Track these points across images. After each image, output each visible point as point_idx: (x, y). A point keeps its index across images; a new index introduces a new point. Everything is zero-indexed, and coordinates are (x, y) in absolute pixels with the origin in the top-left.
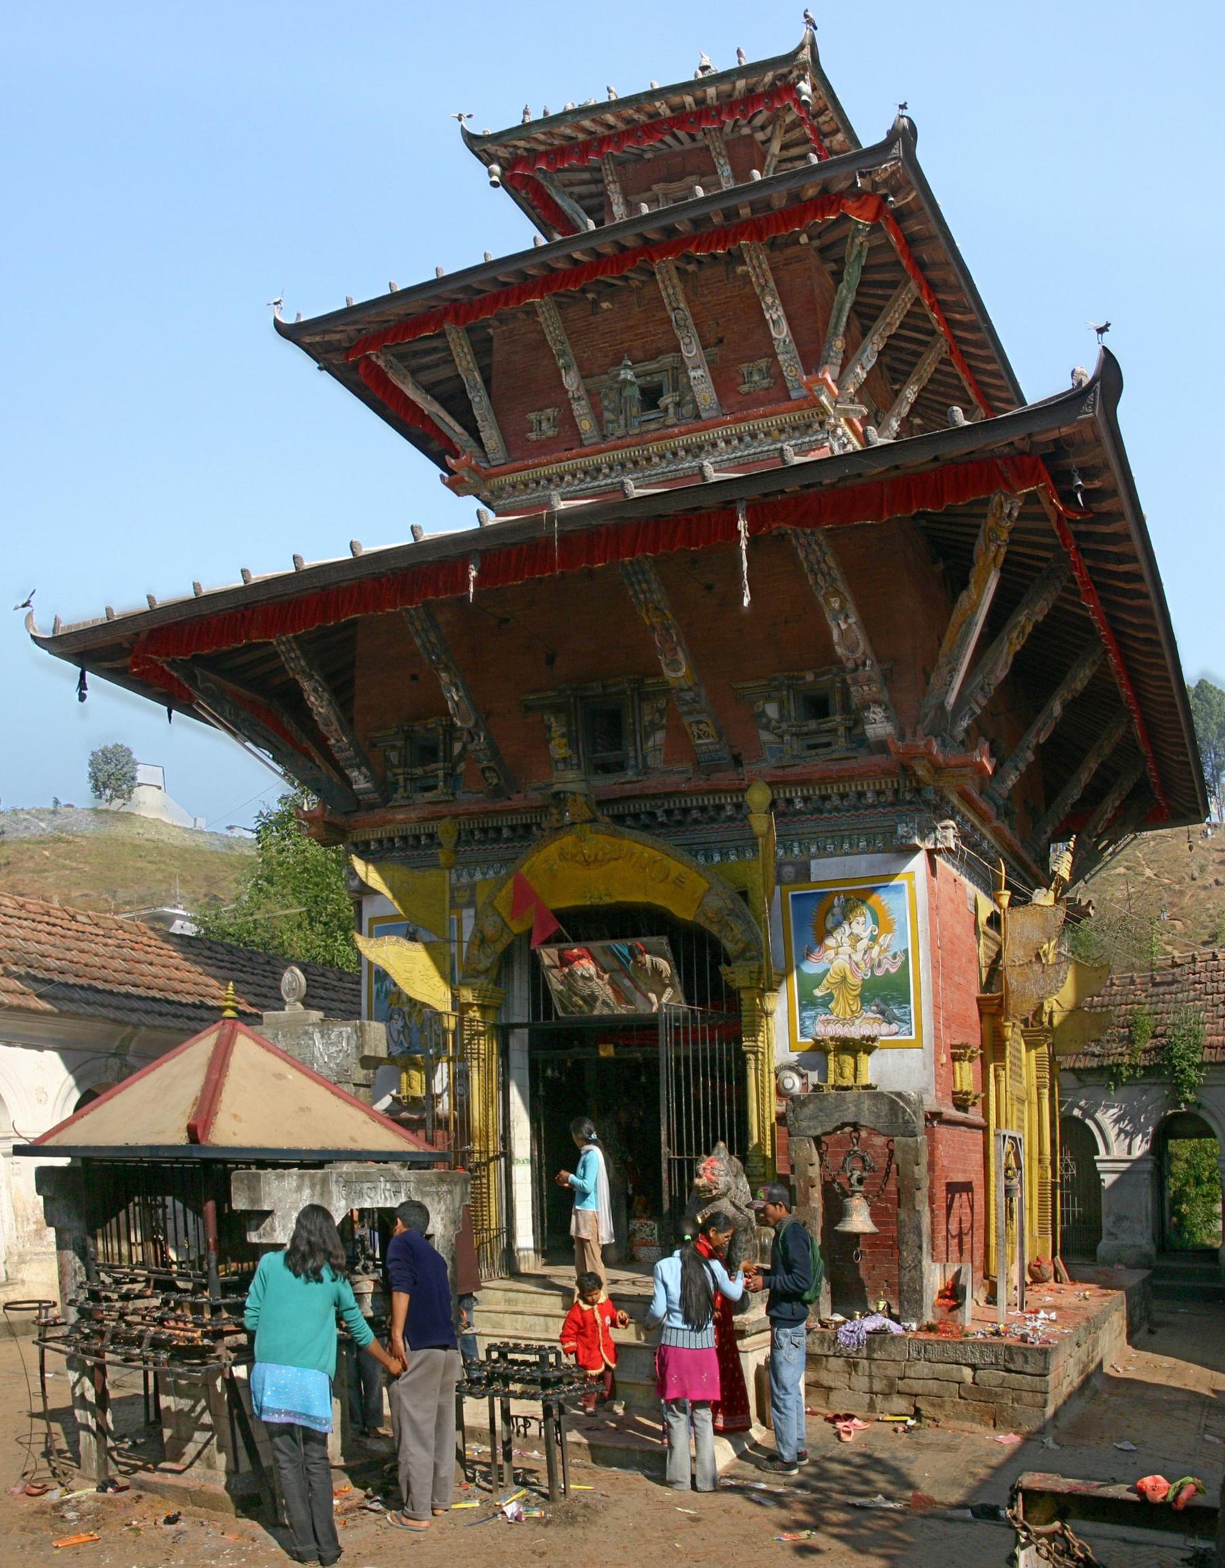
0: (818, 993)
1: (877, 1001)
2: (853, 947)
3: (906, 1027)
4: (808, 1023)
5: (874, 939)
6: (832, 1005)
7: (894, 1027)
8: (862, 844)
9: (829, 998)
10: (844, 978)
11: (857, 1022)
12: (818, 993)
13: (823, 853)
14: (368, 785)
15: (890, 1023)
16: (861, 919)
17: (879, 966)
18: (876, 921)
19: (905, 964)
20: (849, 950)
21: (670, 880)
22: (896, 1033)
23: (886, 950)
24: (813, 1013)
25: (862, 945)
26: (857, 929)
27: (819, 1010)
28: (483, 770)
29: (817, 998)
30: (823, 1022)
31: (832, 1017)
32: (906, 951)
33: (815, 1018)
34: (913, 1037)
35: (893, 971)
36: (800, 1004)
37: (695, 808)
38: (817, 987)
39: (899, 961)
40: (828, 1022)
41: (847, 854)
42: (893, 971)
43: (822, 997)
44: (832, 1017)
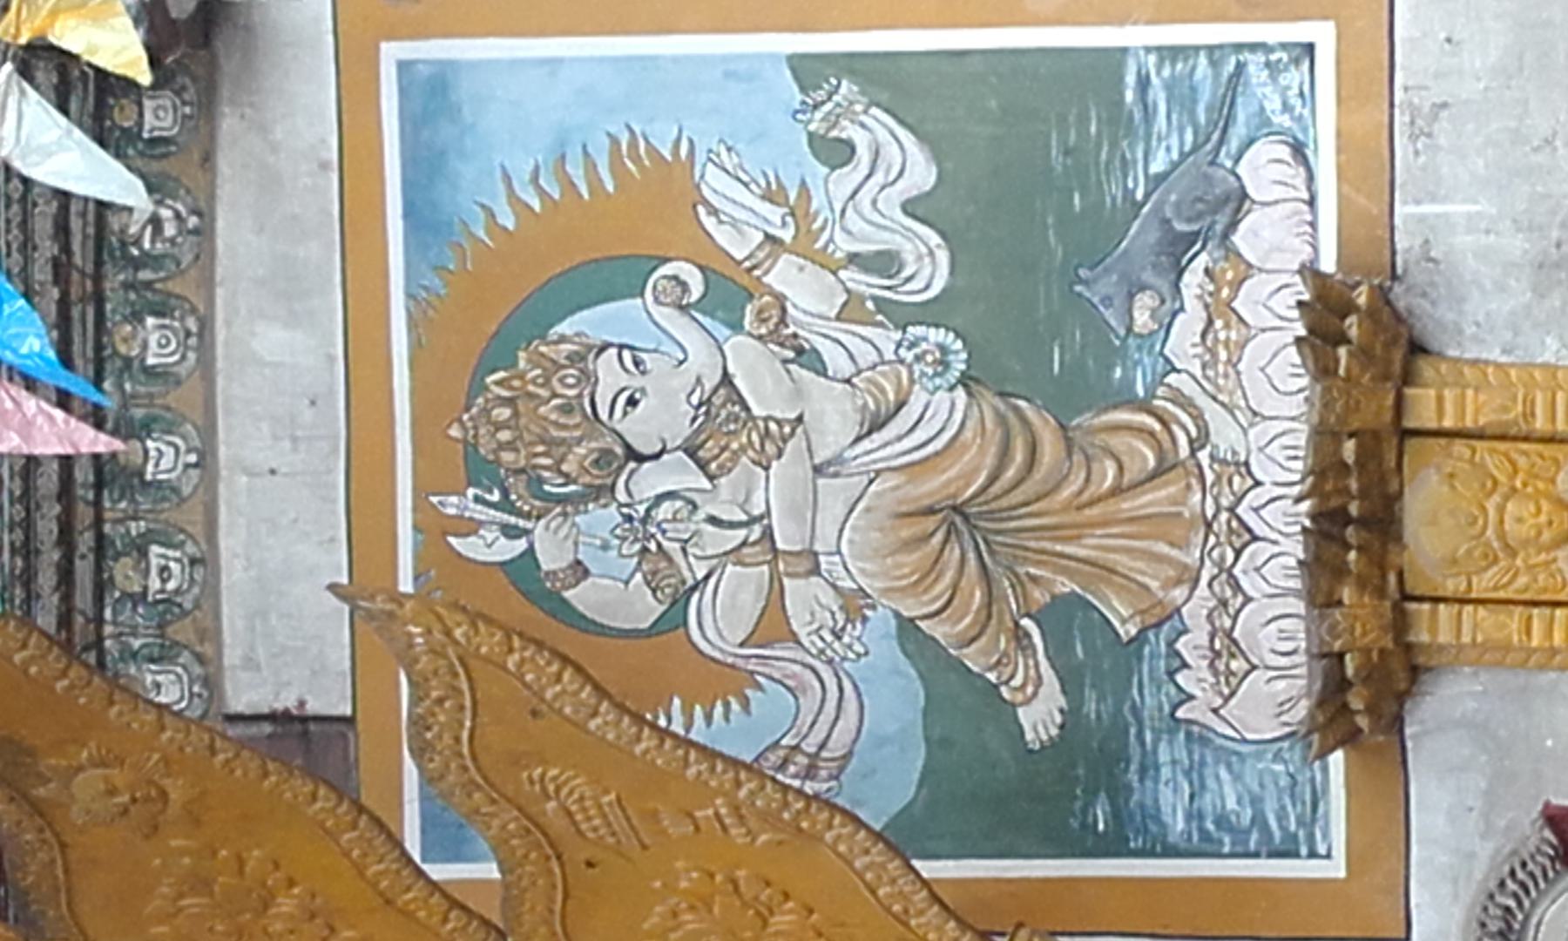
0: (1040, 717)
1: (1099, 289)
2: (774, 439)
3: (1263, 92)
5: (729, 294)
6: (1123, 619)
7: (1262, 169)
8: (155, 343)
9: (1067, 620)
10: (957, 516)
11: (1226, 435)
12: (1040, 717)
13: (186, 628)
15: (1240, 200)
16: (610, 375)
17: (885, 263)
18: (620, 276)
19: (884, 79)
20: (787, 470)
22: (1298, 150)
23: (800, 213)
26: (661, 418)
27: (1152, 702)
29: (1072, 716)
30: (1229, 685)
32: (807, 70)
33: (1198, 737)
34: (1323, 34)
35: (922, 174)
36: (1113, 846)
39: (871, 129)
40: (1225, 646)
41: (206, 461)
42: (922, 174)
44: (1197, 608)
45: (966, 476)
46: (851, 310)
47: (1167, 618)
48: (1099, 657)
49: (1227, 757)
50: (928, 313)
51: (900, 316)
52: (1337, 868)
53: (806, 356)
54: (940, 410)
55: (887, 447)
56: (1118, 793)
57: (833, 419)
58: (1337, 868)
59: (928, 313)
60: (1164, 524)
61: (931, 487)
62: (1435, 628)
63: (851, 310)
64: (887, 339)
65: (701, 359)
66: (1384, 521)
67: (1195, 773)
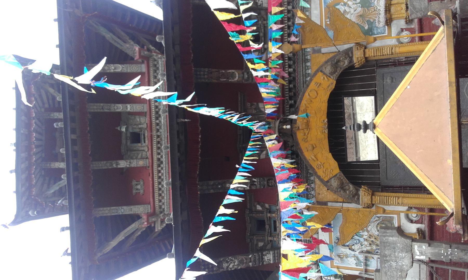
2: (348, 13)
4: (379, 31)
6: (372, 20)
9: (368, 21)
10: (361, 16)
11: (379, 8)
12: (366, 28)
14: (271, 253)
21: (316, 89)
24: (375, 29)
25: (347, 10)
27: (374, 25)
28: (268, 186)
29: (369, 27)
30: (379, 24)
31: (377, 19)
33: (377, 27)
37: (289, 85)
38: (364, 28)
40: (379, 21)
43: (368, 25)
44: (377, 19)
45: (361, 13)
46: (353, 4)
47: (375, 20)
48: (371, 23)
49: (379, 28)
50: (359, 3)
51: (356, 4)
52: (387, 34)
53: (350, 7)
54: (359, 9)
55: (356, 12)
56: (372, 32)
57: (352, 11)
58: (387, 34)
59: (359, 3)
60: (375, 14)
61: (359, 14)
62: (393, 16)
63: (353, 4)
64: (356, 5)
65: (343, 9)
66: (390, 11)
67: (377, 30)
